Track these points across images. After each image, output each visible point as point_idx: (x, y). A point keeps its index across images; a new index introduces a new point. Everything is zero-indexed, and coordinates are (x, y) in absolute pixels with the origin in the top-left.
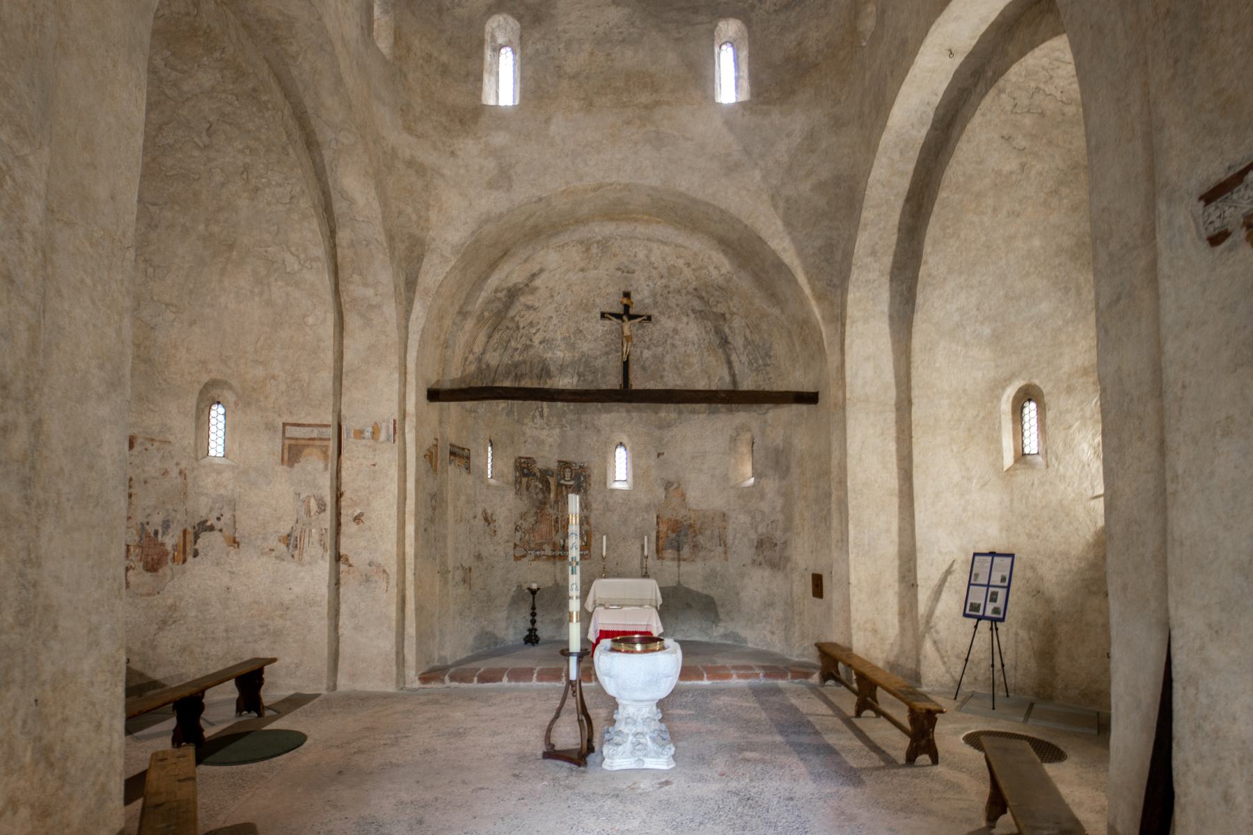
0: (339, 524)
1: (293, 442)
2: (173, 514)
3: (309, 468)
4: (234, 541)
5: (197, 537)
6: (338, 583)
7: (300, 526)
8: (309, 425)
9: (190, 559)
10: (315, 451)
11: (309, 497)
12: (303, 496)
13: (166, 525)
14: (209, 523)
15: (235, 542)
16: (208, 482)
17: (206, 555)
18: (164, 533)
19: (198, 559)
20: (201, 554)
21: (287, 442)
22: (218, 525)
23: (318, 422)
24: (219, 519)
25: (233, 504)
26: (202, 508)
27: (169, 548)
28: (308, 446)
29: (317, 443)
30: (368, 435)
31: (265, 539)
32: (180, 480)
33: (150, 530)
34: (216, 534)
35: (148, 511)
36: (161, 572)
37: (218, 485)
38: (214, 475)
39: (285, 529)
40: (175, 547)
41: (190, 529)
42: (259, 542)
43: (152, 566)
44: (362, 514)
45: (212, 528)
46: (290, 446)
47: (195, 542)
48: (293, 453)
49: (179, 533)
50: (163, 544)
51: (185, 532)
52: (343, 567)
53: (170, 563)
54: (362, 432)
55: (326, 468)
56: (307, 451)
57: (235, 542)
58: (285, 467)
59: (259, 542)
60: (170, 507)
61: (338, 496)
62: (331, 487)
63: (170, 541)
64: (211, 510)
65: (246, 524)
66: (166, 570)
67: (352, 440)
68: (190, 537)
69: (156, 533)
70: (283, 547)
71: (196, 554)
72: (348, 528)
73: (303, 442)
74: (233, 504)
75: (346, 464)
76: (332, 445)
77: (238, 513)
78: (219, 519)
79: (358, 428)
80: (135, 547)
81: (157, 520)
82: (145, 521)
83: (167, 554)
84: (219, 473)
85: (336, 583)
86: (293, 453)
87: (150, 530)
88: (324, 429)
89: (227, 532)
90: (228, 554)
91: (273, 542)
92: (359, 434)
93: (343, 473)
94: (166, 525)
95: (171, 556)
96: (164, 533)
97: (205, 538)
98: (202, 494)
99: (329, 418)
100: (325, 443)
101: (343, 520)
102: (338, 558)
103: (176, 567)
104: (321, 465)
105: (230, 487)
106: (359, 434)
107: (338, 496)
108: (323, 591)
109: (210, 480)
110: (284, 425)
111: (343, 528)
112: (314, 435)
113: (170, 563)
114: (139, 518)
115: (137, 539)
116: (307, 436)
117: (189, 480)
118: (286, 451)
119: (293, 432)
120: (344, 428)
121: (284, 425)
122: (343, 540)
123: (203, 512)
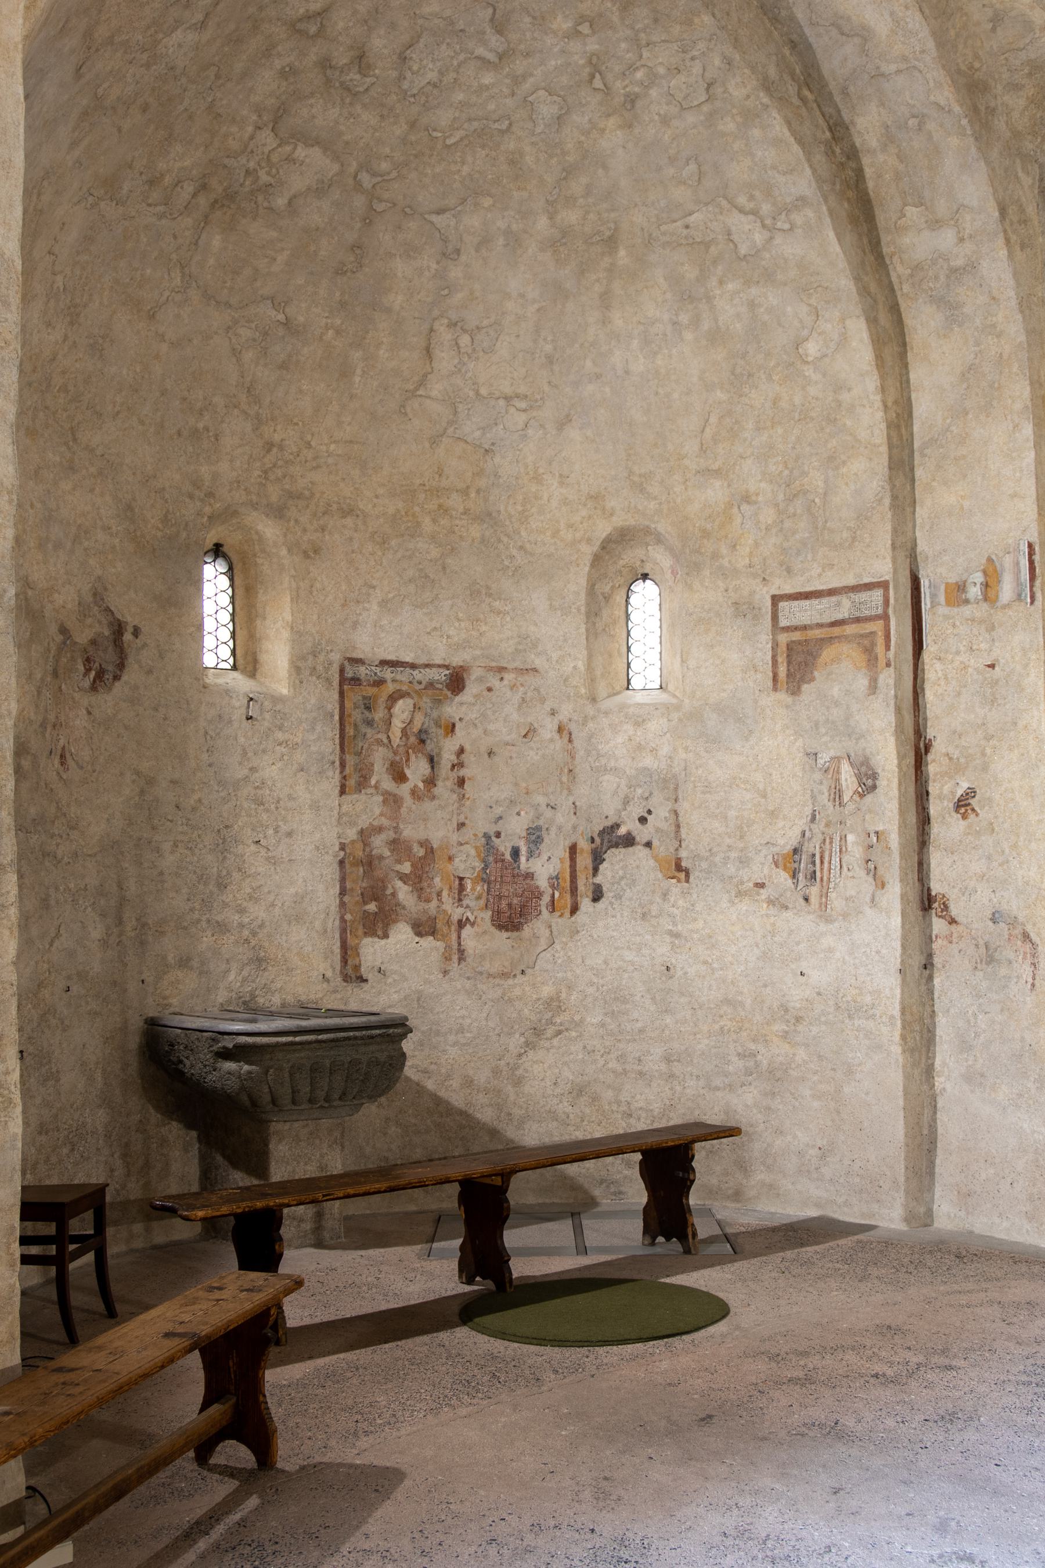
0: (924, 820)
1: (796, 636)
2: (548, 813)
3: (836, 691)
4: (679, 868)
5: (598, 859)
6: (928, 965)
7: (818, 828)
8: (831, 592)
9: (586, 904)
10: (845, 648)
11: (837, 759)
12: (824, 758)
13: (535, 837)
14: (622, 831)
15: (679, 870)
16: (616, 744)
17: (618, 897)
18: (531, 854)
19: (601, 905)
20: (608, 895)
21: (783, 638)
22: (642, 833)
23: (851, 580)
24: (643, 820)
25: (672, 786)
26: (607, 799)
27: (542, 883)
28: (831, 639)
29: (850, 629)
30: (974, 592)
31: (744, 861)
32: (560, 744)
33: (504, 847)
34: (639, 851)
35: (499, 810)
36: (527, 931)
37: (640, 747)
38: (629, 728)
39: (787, 837)
40: (555, 881)
41: (584, 845)
42: (731, 869)
43: (511, 920)
44: (971, 793)
45: (629, 841)
46: (790, 647)
47: (596, 870)
48: (797, 662)
49: (562, 852)
50: (529, 876)
51: (573, 849)
52: (938, 925)
53: (545, 912)
54: (961, 587)
55: (873, 687)
56: (827, 653)
57: (679, 870)
58: (782, 696)
59: (731, 869)
60: (541, 800)
61: (919, 751)
62: (899, 730)
63: (544, 868)
64: (626, 801)
65: (702, 830)
66: (537, 927)
67: (943, 610)
68: (584, 861)
69: (516, 853)
70: (783, 878)
71: (597, 895)
72: (946, 826)
73: (817, 633)
74: (672, 786)
75: (933, 670)
76: (900, 627)
77: (684, 806)
78: (643, 820)
79: (953, 579)
80: (475, 881)
81: (515, 828)
82: (492, 830)
83: (539, 896)
84: (639, 722)
85: (922, 966)
86: (797, 662)
87: (504, 847)
88: (863, 596)
89: (664, 848)
90: (665, 895)
91: (761, 868)
92: (957, 593)
93: (930, 695)
94: (535, 837)
95: (546, 899)
96: (531, 854)
97: (615, 860)
98: (606, 770)
99: (882, 566)
100: (869, 627)
101: (933, 811)
102: (927, 902)
103: (560, 922)
104: (862, 682)
105: (665, 750)
106: (957, 593)
107: (919, 751)
108: (887, 987)
109: (620, 739)
110: (776, 599)
111: (936, 829)
112: (843, 613)
113: (545, 912)
114: (481, 824)
115: (479, 865)
116: (826, 619)
117: (578, 743)
118: (782, 659)
119: (795, 613)
120: (924, 583)
121: (776, 599)
122: (936, 860)
123: (610, 808)
